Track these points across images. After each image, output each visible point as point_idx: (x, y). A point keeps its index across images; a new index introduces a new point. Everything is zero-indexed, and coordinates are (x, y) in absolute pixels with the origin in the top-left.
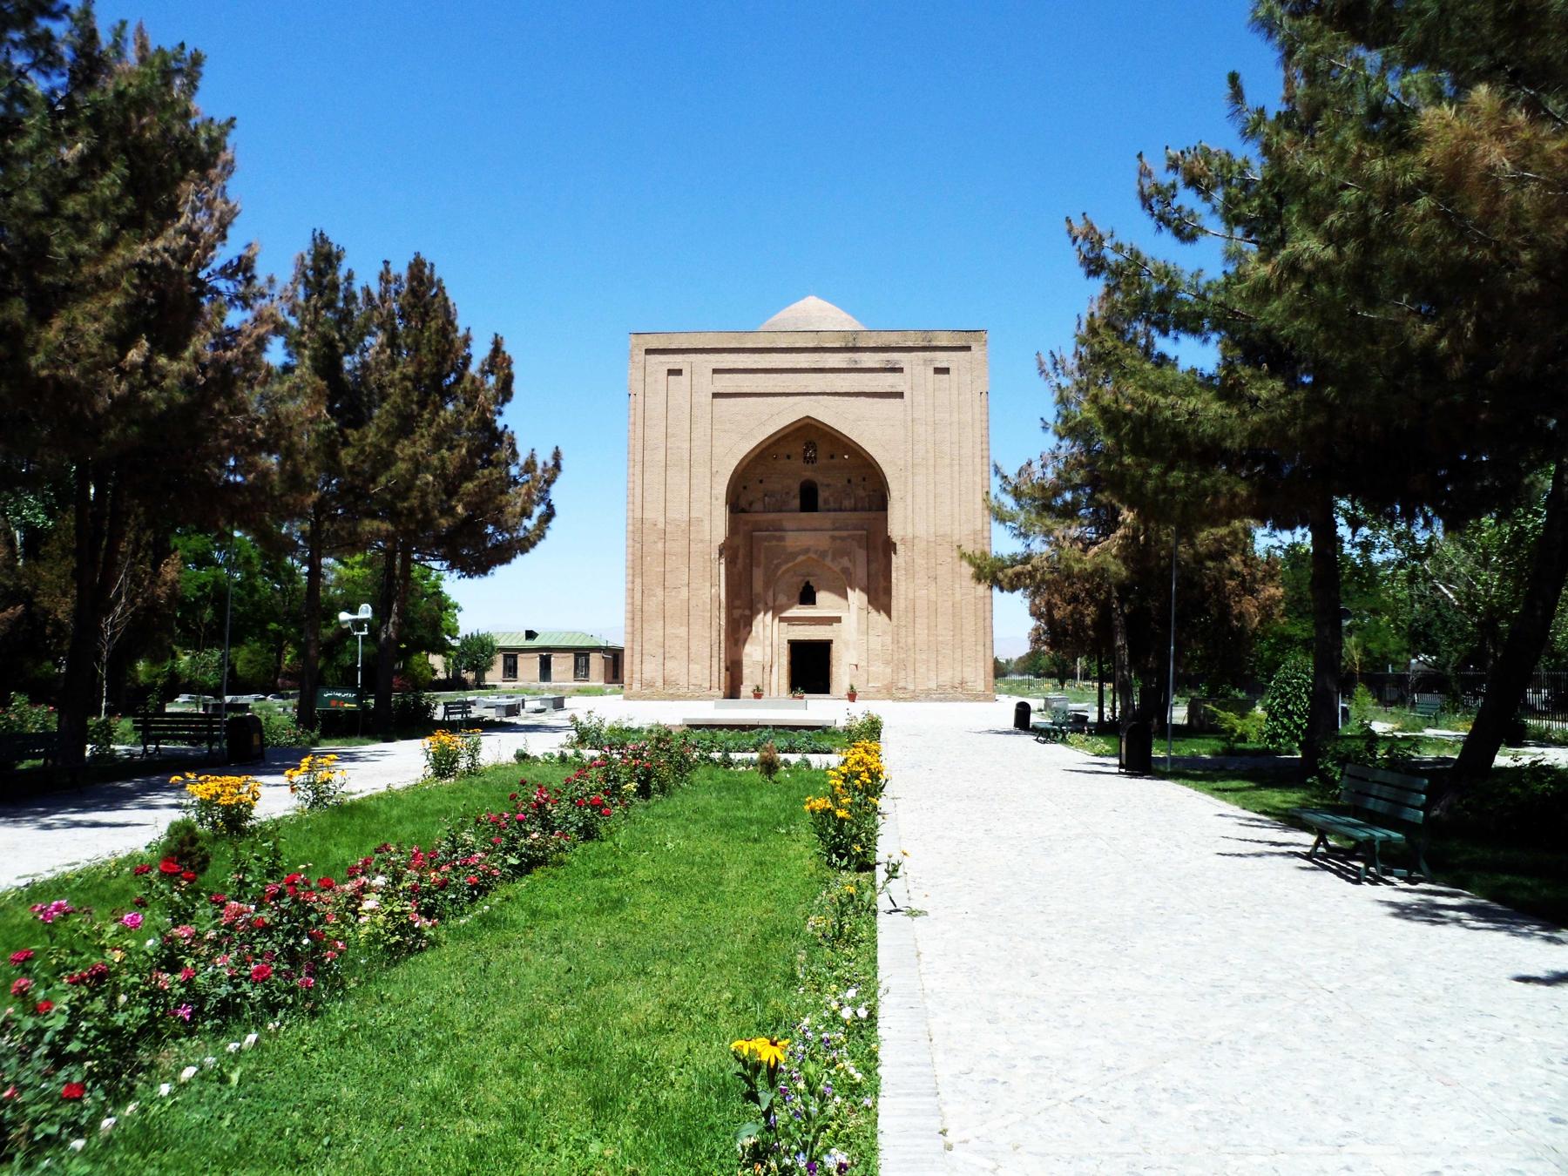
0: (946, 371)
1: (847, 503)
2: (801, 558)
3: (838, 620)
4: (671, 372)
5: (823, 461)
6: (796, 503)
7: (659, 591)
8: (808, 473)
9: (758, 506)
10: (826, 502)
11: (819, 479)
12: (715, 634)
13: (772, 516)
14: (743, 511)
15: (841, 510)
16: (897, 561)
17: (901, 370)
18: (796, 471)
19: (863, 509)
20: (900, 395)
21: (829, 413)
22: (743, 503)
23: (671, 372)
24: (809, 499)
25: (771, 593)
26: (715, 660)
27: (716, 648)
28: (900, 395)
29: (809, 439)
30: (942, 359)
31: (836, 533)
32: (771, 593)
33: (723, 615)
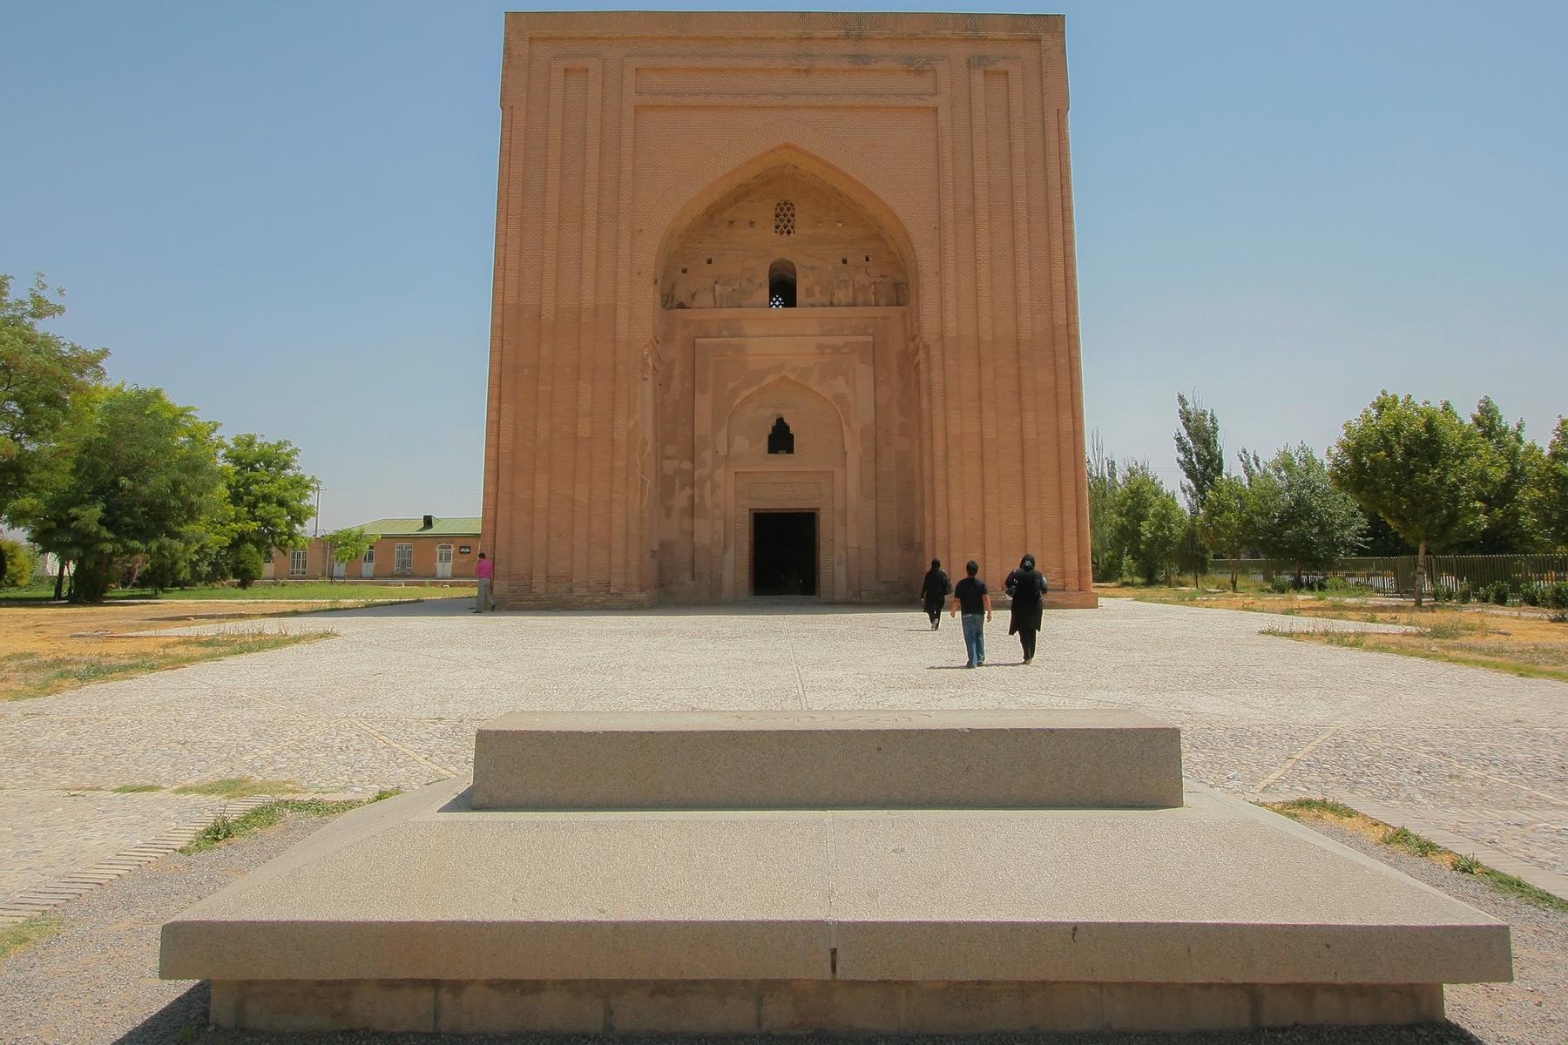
1: (842, 295)
2: (770, 379)
5: (802, 229)
8: (783, 249)
10: (809, 293)
11: (800, 261)
13: (727, 313)
14: (682, 306)
15: (832, 305)
18: (760, 247)
19: (867, 304)
22: (681, 295)
24: (784, 289)
25: (723, 435)
29: (782, 193)
31: (827, 340)
32: (723, 435)
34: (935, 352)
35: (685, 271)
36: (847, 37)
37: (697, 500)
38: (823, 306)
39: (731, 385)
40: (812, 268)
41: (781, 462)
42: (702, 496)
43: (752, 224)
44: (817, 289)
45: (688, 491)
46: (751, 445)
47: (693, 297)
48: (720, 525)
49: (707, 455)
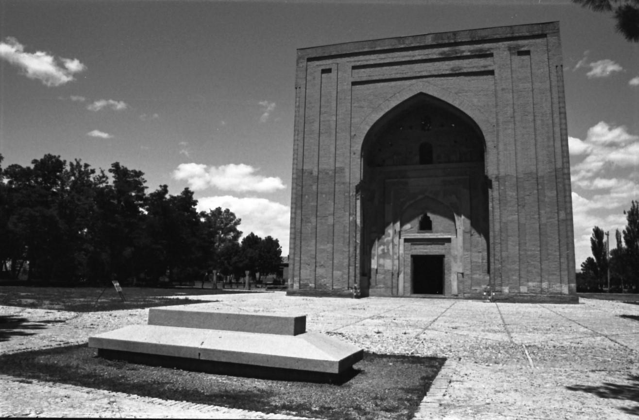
0: (527, 53)
2: (420, 197)
3: (449, 240)
4: (324, 71)
7: (313, 219)
12: (352, 249)
16: (493, 194)
17: (491, 55)
20: (492, 73)
21: (434, 89)
23: (324, 71)
24: (426, 156)
26: (352, 268)
27: (352, 260)
28: (492, 73)
29: (423, 111)
30: (524, 44)
33: (358, 236)
34: (495, 184)
37: (386, 251)
42: (388, 249)
45: (382, 247)
48: (396, 262)
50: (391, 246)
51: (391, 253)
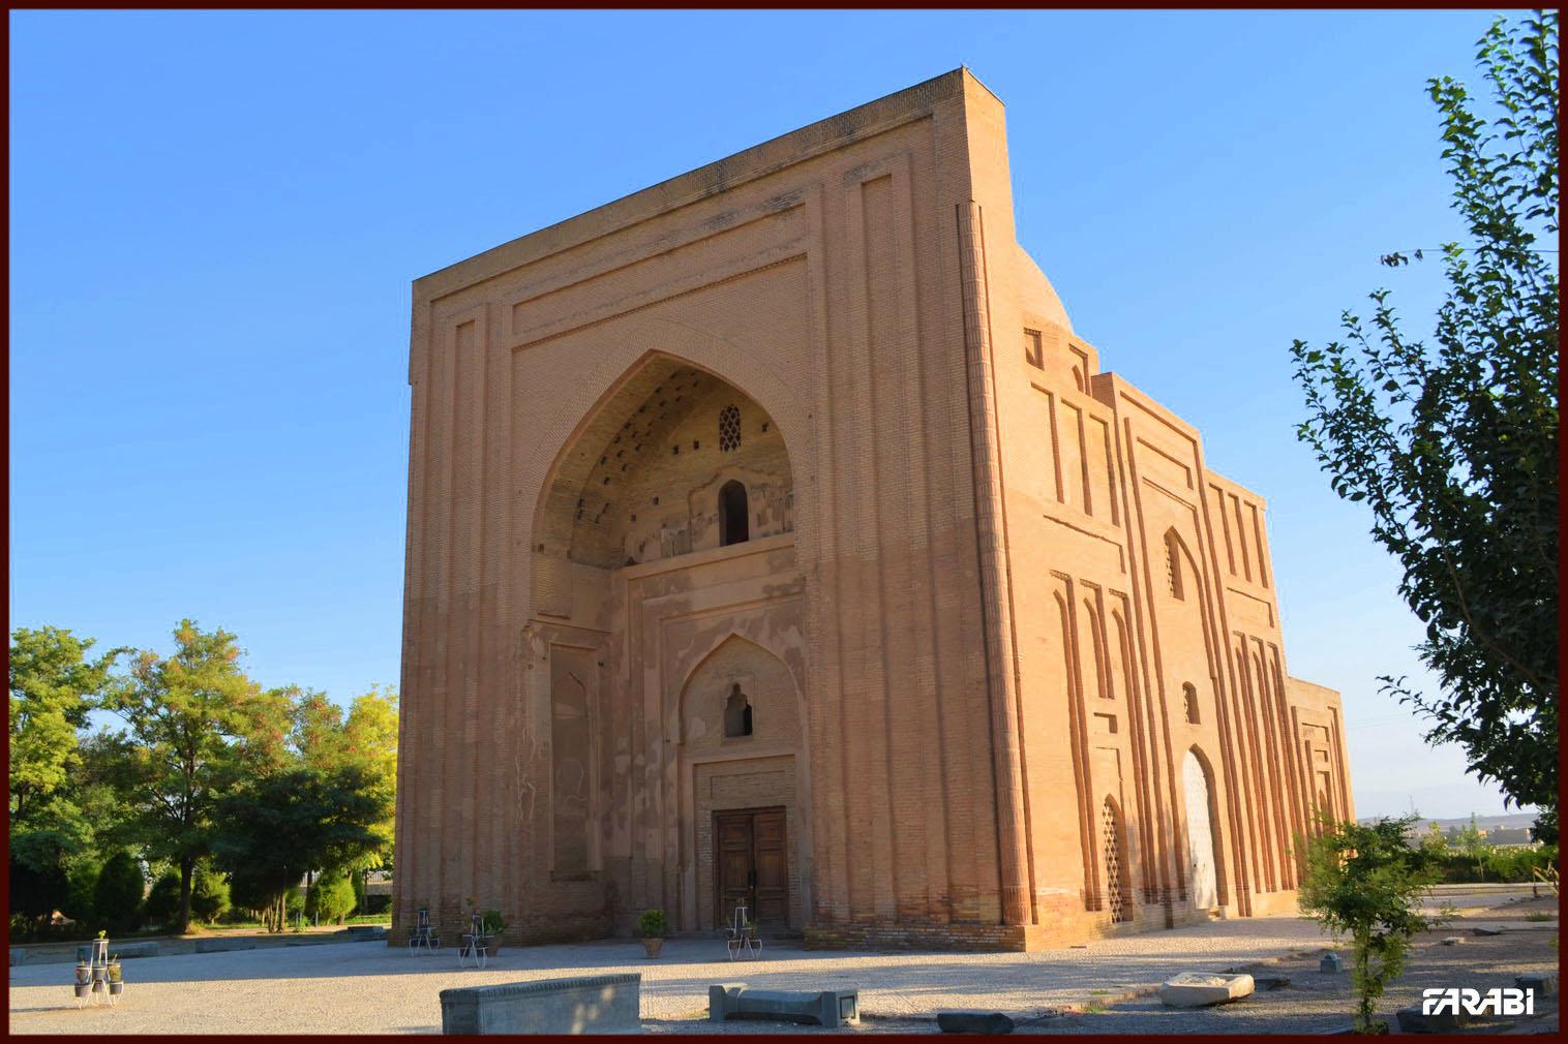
2: (720, 639)
6: (714, 531)
9: (653, 550)
10: (761, 520)
14: (631, 563)
35: (634, 518)
36: (710, 196)
37: (648, 804)
38: (777, 533)
39: (681, 654)
40: (764, 486)
41: (743, 749)
42: (653, 799)
43: (696, 445)
44: (769, 512)
46: (706, 728)
47: (641, 549)
49: (657, 746)
50: (659, 783)
51: (659, 809)
